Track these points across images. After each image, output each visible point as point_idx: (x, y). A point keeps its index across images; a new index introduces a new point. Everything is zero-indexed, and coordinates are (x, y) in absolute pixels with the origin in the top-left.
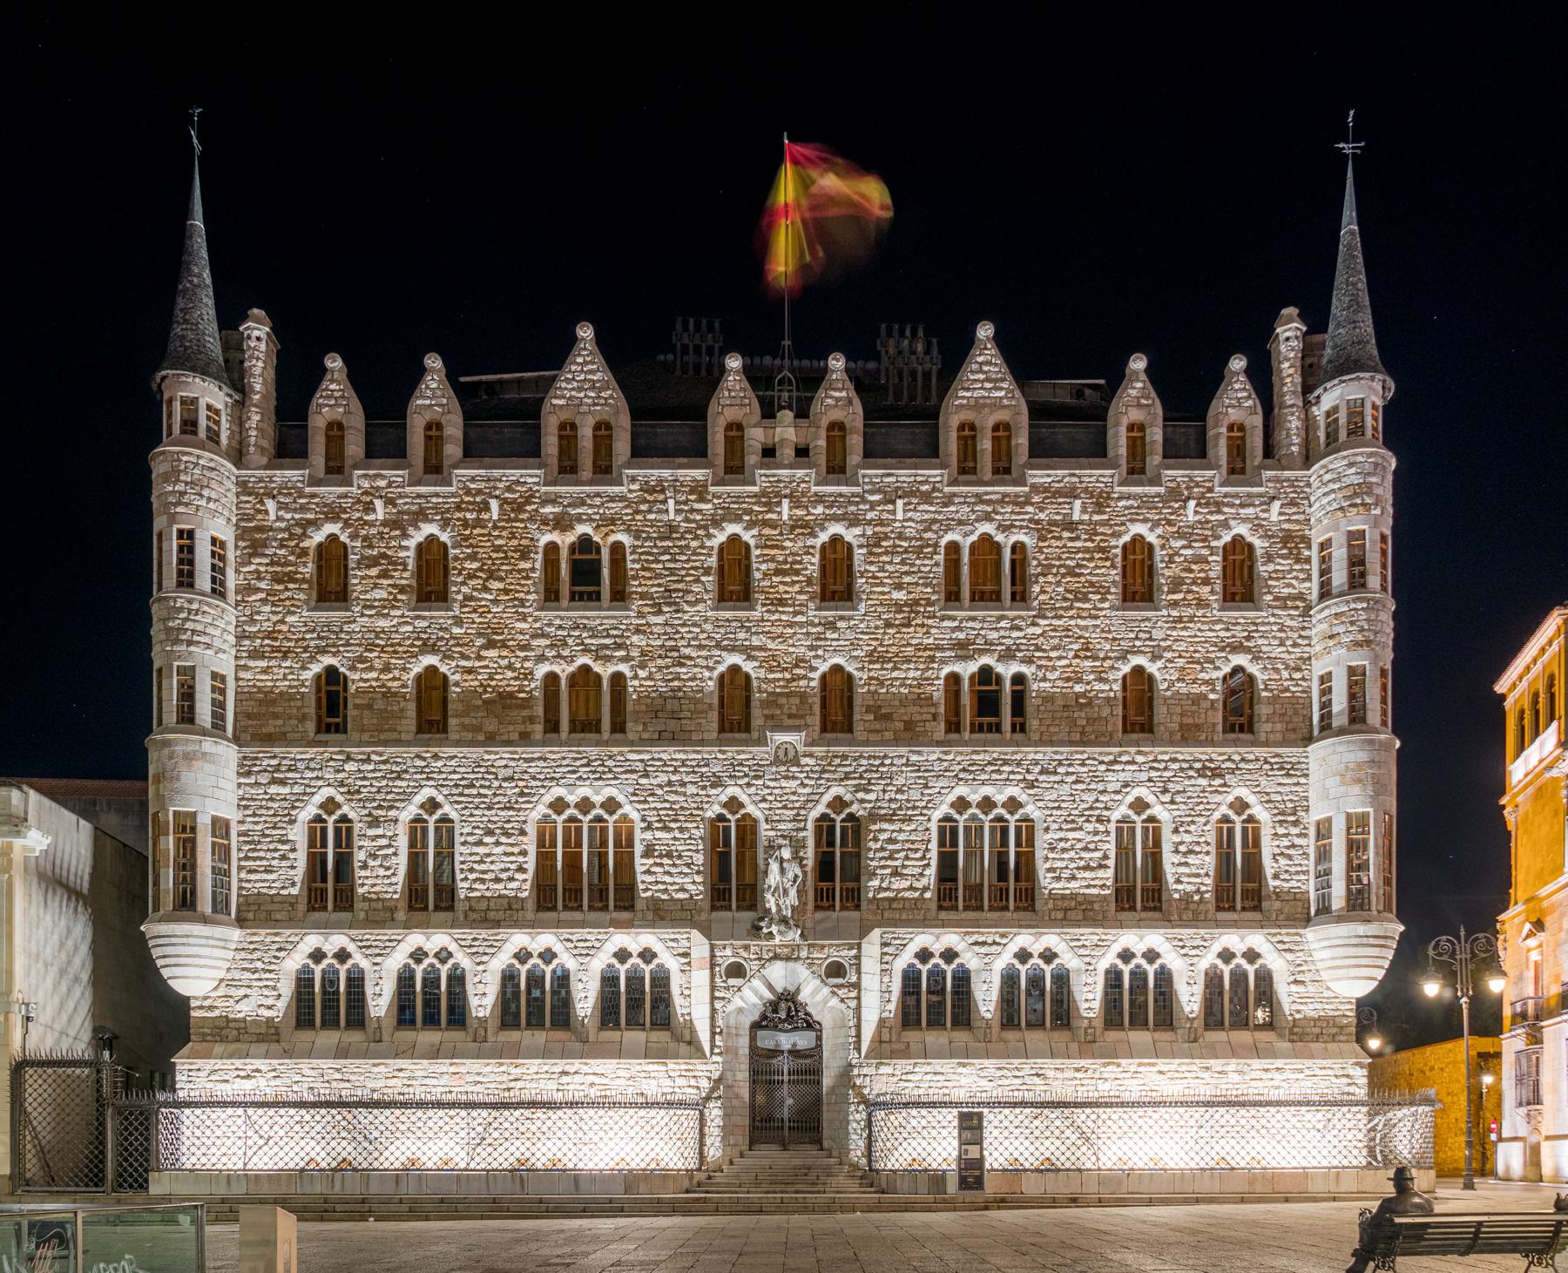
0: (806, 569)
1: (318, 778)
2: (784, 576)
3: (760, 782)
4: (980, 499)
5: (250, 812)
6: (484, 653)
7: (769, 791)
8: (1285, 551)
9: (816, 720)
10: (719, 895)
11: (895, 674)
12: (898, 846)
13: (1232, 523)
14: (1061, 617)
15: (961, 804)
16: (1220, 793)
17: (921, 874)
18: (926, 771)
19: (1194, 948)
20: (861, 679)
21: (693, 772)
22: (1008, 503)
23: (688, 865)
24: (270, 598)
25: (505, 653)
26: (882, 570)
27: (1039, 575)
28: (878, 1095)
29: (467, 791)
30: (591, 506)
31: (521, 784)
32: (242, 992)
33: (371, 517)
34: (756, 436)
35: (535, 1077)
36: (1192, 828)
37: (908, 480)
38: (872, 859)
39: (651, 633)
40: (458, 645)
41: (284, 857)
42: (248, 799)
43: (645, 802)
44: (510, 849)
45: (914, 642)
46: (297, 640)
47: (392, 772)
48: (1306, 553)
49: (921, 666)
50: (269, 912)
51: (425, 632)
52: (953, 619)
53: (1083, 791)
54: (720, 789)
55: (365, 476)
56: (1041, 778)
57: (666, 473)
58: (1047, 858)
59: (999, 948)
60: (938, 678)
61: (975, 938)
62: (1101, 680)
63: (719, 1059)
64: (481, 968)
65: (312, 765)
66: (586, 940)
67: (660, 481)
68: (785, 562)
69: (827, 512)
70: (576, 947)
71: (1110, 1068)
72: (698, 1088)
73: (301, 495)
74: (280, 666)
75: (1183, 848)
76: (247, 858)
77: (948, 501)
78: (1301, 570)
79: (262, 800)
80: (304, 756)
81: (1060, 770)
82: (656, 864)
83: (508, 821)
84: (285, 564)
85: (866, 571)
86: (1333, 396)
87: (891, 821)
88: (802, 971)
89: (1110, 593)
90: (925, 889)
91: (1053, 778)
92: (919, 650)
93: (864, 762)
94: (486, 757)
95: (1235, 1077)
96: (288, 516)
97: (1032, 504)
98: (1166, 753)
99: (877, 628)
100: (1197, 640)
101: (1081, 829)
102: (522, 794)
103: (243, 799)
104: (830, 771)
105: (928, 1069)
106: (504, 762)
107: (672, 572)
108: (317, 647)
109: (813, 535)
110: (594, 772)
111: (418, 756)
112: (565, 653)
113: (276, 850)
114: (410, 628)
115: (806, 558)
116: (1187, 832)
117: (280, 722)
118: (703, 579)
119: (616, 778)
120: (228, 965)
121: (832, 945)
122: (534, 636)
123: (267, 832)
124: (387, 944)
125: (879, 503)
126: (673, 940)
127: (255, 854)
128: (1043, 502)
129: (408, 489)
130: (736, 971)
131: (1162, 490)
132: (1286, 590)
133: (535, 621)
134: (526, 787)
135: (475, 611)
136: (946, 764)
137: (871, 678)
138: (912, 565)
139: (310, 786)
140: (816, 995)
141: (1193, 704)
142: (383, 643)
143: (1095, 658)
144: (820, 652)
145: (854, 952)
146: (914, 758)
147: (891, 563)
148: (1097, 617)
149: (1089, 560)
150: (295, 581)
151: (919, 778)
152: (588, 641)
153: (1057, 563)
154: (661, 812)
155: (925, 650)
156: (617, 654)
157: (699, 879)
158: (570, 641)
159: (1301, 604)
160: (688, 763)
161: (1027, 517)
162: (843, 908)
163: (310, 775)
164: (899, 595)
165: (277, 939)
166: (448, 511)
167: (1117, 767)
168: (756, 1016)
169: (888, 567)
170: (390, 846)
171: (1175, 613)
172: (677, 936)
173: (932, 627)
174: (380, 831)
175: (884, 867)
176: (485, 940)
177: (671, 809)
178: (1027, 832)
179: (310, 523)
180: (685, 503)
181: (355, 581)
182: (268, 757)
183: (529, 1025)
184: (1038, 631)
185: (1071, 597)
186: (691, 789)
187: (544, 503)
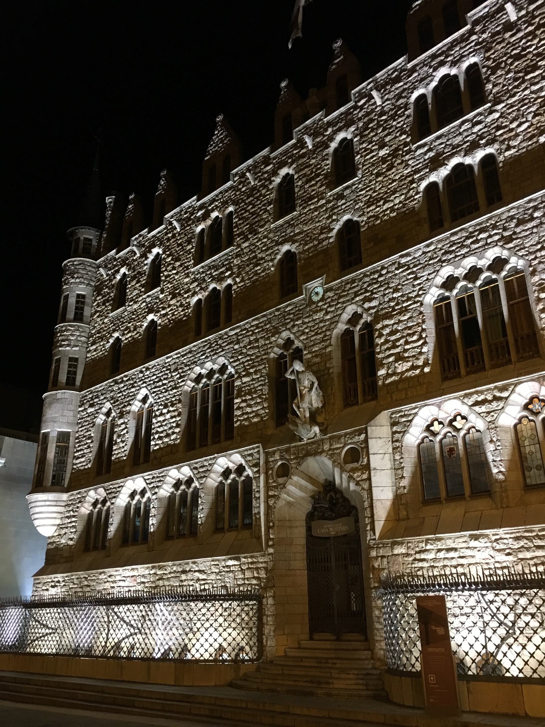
0: (324, 170)
1: (105, 398)
2: (311, 182)
4: (434, 56)
5: (80, 426)
6: (172, 302)
7: (305, 326)
17: (421, 353)
18: (415, 266)
20: (363, 221)
21: (263, 330)
22: (456, 46)
23: (259, 397)
25: (179, 299)
27: (490, 75)
28: (396, 578)
29: (158, 384)
31: (180, 371)
32: (63, 532)
35: (169, 576)
37: (384, 77)
38: (379, 353)
39: (243, 254)
40: (162, 303)
43: (238, 360)
44: (174, 414)
49: (405, 191)
54: (277, 336)
56: (518, 230)
59: (501, 404)
60: (418, 193)
61: (475, 398)
63: (271, 550)
64: (154, 497)
65: (104, 392)
66: (204, 466)
69: (335, 129)
70: (199, 472)
72: (258, 578)
73: (115, 260)
81: (536, 215)
82: (243, 401)
83: (174, 396)
90: (426, 364)
91: (530, 225)
92: (401, 181)
93: (367, 279)
94: (167, 361)
96: (110, 272)
97: (475, 33)
102: (181, 377)
103: (80, 419)
104: (344, 296)
105: (440, 545)
106: (174, 361)
107: (253, 214)
110: (212, 351)
111: (141, 372)
114: (144, 304)
118: (268, 208)
119: (223, 350)
121: (345, 435)
124: (118, 489)
126: (251, 455)
128: (484, 26)
134: (182, 372)
135: (169, 282)
136: (429, 254)
137: (368, 218)
138: (392, 126)
142: (134, 317)
144: (334, 217)
145: (363, 436)
146: (403, 261)
147: (376, 135)
151: (409, 274)
153: (504, 59)
154: (246, 364)
155: (405, 179)
156: (227, 274)
158: (206, 278)
160: (260, 325)
161: (473, 44)
162: (365, 401)
163: (102, 398)
164: (382, 153)
165: (79, 496)
166: (163, 238)
168: (308, 507)
169: (375, 139)
170: (126, 428)
172: (251, 451)
173: (409, 160)
174: (122, 421)
176: (158, 477)
177: (251, 360)
180: (259, 172)
184: (497, 115)
185: (521, 75)
186: (262, 342)
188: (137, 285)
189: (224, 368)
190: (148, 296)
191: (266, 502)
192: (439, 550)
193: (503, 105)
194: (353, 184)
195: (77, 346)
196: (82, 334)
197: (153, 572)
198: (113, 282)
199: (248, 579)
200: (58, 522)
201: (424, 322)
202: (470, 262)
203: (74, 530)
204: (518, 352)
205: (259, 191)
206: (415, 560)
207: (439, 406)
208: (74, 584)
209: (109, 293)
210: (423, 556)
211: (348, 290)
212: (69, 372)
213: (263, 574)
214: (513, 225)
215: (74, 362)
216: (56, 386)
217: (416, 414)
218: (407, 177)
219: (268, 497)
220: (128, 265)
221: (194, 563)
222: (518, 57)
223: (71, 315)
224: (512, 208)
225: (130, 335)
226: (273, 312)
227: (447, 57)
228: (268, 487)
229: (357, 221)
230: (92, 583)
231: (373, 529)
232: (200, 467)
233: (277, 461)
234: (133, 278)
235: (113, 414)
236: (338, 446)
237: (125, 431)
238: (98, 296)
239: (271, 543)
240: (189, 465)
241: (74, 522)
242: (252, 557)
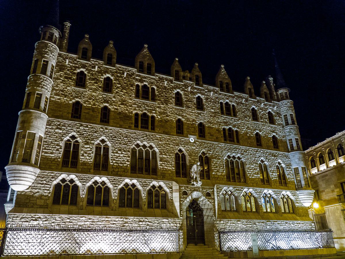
1: (71, 129)
3: (187, 146)
4: (225, 95)
5: (48, 136)
9: (197, 134)
10: (178, 173)
11: (213, 126)
12: (218, 165)
14: (243, 121)
15: (229, 157)
21: (172, 142)
23: (171, 165)
25: (126, 107)
26: (209, 105)
28: (221, 229)
29: (114, 139)
30: (147, 79)
31: (129, 139)
33: (94, 70)
34: (182, 74)
35: (132, 222)
36: (273, 167)
38: (213, 167)
41: (57, 150)
42: (48, 132)
43: (160, 147)
44: (125, 155)
45: (216, 120)
46: (69, 94)
47: (93, 131)
50: (50, 166)
51: (105, 98)
52: (223, 117)
55: (93, 61)
56: (244, 153)
57: (164, 76)
58: (248, 171)
62: (252, 134)
63: (181, 218)
64: (116, 188)
65: (70, 126)
67: (163, 78)
70: (143, 184)
71: (268, 223)
72: (176, 226)
74: (64, 99)
76: (45, 149)
77: (220, 94)
79: (53, 133)
80: (68, 123)
82: (163, 163)
83: (125, 148)
84: (69, 75)
86: (281, 91)
87: (216, 159)
88: (200, 194)
93: (209, 145)
94: (120, 131)
95: (292, 225)
96: (71, 64)
99: (209, 116)
101: (253, 165)
102: (129, 141)
107: (166, 96)
108: (75, 96)
110: (148, 138)
111: (102, 128)
112: (141, 109)
113: (55, 148)
114: (101, 96)
115: (194, 99)
117: (61, 113)
119: (153, 141)
121: (207, 188)
122: (133, 104)
123: (53, 142)
124: (88, 179)
126: (168, 184)
127: (48, 148)
129: (104, 66)
130: (185, 193)
131: (256, 100)
133: (134, 101)
139: (69, 131)
140: (203, 201)
142: (94, 98)
143: (250, 130)
144: (198, 119)
146: (219, 145)
149: (247, 111)
150: (71, 79)
152: (146, 108)
156: (153, 112)
157: (173, 168)
165: (52, 174)
166: (113, 72)
170: (91, 151)
174: (88, 146)
175: (216, 170)
176: (117, 180)
178: (243, 164)
179: (77, 67)
181: (88, 83)
182: (56, 121)
183: (127, 206)
186: (171, 146)
187: (137, 76)
188: (96, 84)
192: (231, 223)
194: (203, 113)
197: (122, 219)
198: (75, 72)
200: (30, 184)
202: (234, 154)
203: (49, 192)
208: (56, 220)
210: (227, 224)
213: (178, 225)
215: (47, 98)
217: (223, 188)
218: (219, 122)
219: (180, 201)
221: (146, 219)
222: (243, 112)
225: (90, 105)
229: (85, 74)
230: (73, 221)
232: (143, 182)
237: (91, 152)
239: (181, 215)
241: (47, 187)
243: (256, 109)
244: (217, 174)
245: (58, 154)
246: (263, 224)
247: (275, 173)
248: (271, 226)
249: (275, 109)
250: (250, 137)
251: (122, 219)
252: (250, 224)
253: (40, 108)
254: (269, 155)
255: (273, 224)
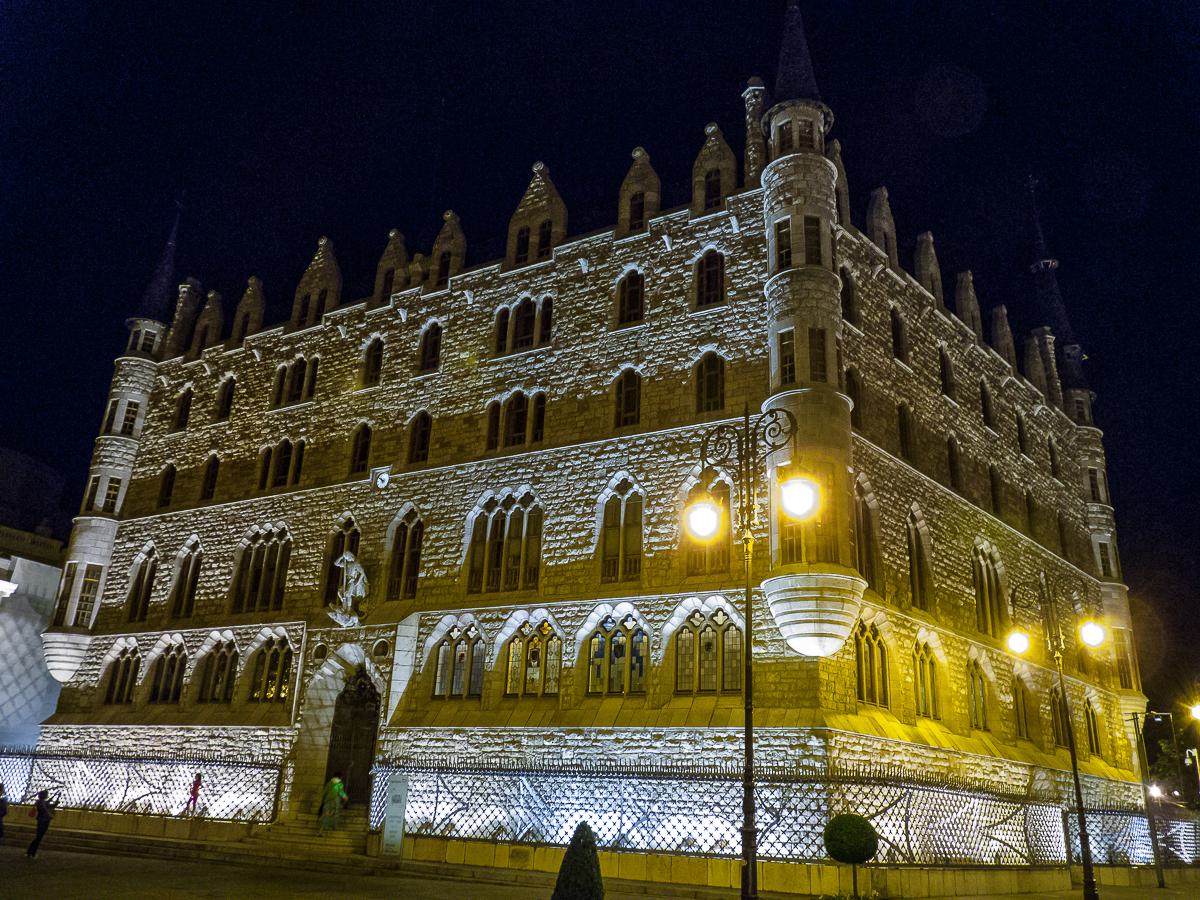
1: (148, 535)
4: (522, 276)
6: (239, 443)
8: (745, 254)
9: (405, 455)
13: (702, 243)
14: (568, 346)
16: (687, 465)
18: (466, 482)
19: (658, 613)
23: (313, 573)
24: (156, 432)
25: (247, 441)
26: (456, 340)
31: (238, 525)
32: (82, 679)
34: (399, 274)
35: (197, 739)
36: (662, 500)
38: (423, 556)
41: (122, 588)
43: (298, 529)
48: (765, 250)
52: (496, 364)
53: (575, 480)
55: (209, 352)
56: (545, 475)
58: (546, 541)
62: (597, 388)
63: (298, 725)
64: (191, 657)
65: (148, 527)
67: (343, 315)
68: (400, 350)
71: (572, 736)
72: (283, 750)
75: (654, 520)
76: (109, 590)
77: (502, 282)
78: (759, 265)
83: (227, 552)
85: (447, 343)
89: (607, 320)
92: (472, 391)
93: (427, 481)
95: (687, 747)
97: (556, 270)
98: (642, 438)
100: (673, 340)
101: (573, 513)
102: (237, 532)
103: (115, 552)
104: (405, 491)
107: (338, 371)
109: (419, 328)
110: (274, 512)
111: (195, 515)
114: (208, 435)
116: (658, 504)
118: (354, 371)
119: (285, 514)
120: (82, 660)
121: (379, 628)
122: (264, 428)
125: (458, 296)
126: (294, 630)
129: (224, 354)
130: (322, 653)
131: (648, 234)
132: (747, 284)
141: (670, 393)
143: (592, 372)
144: (411, 406)
145: (393, 632)
148: (596, 340)
149: (593, 299)
151: (461, 487)
159: (760, 292)
162: (405, 598)
165: (105, 642)
167: (603, 457)
170: (169, 575)
171: (656, 324)
189: (282, 534)
190: (214, 428)
191: (301, 680)
192: (431, 740)
193: (560, 352)
195: (122, 465)
196: (130, 452)
197: (181, 733)
198: (175, 397)
199: (273, 750)
200: (77, 667)
201: (463, 536)
202: (506, 491)
204: (525, 581)
205: (348, 348)
206: (412, 745)
207: (458, 616)
208: (91, 737)
209: (168, 409)
210: (419, 744)
211: (409, 487)
212: (108, 496)
213: (287, 747)
214: (542, 469)
215: (115, 482)
216: (90, 510)
217: (440, 620)
219: (304, 675)
220: (195, 381)
221: (224, 729)
222: (580, 311)
223: (118, 427)
224: (545, 454)
225: (186, 467)
226: (340, 488)
227: (531, 283)
228: (306, 666)
230: (111, 739)
231: (385, 717)
233: (317, 642)
234: (200, 399)
235: (156, 555)
236: (372, 637)
237: (167, 579)
238: (154, 408)
240: (232, 630)
241: (95, 669)
242: (280, 730)
243: (640, 271)
244: (432, 577)
245: (122, 596)
246: (547, 743)
247: (665, 523)
248: (581, 751)
249: (736, 231)
250: (584, 406)
251: (181, 733)
252: (497, 744)
253: (95, 507)
254: (655, 450)
255: (596, 740)
